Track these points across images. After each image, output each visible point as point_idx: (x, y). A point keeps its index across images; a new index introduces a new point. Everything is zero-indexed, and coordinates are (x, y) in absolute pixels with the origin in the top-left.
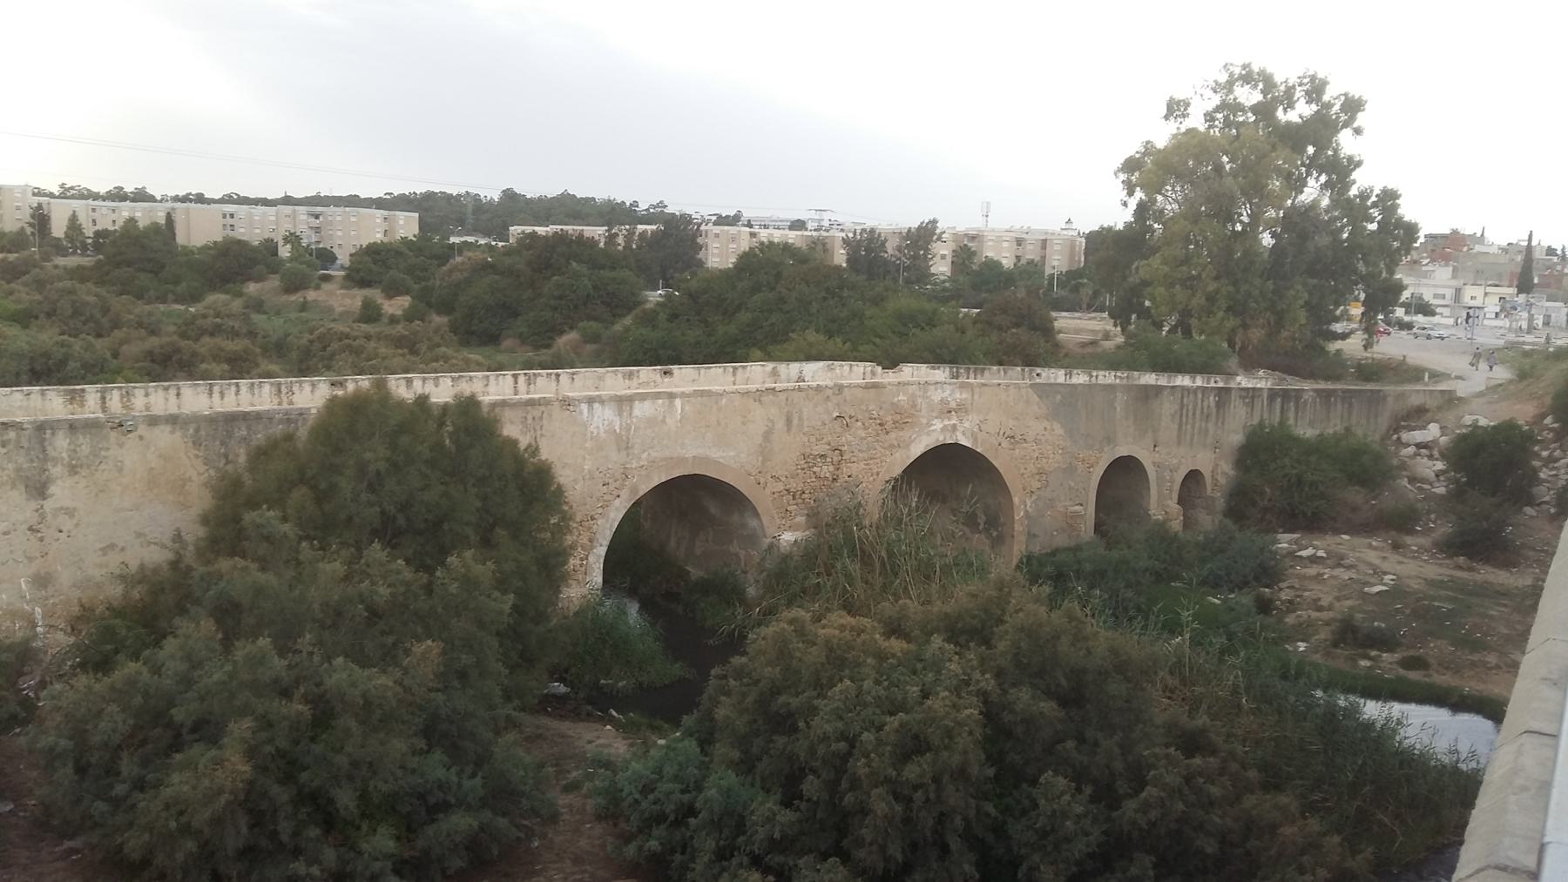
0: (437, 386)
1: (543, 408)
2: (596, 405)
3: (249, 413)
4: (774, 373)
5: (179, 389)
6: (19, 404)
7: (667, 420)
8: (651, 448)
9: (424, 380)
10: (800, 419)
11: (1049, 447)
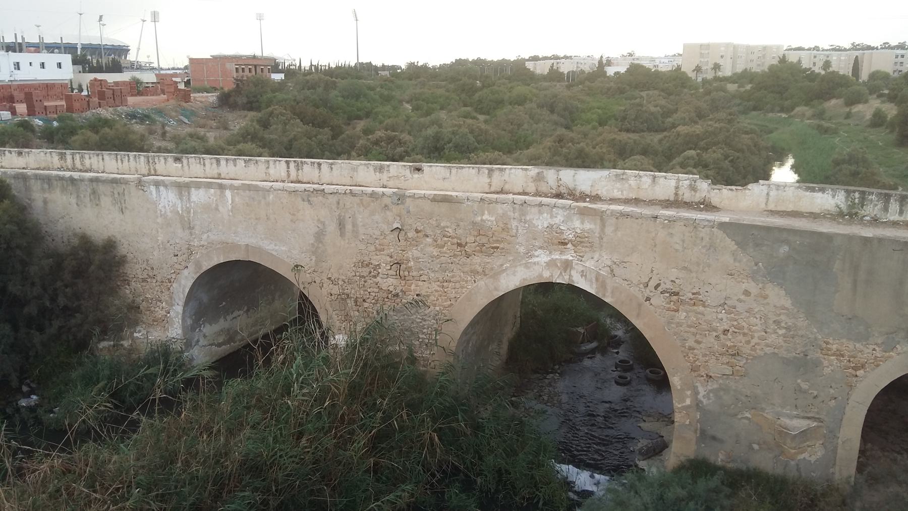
0: (235, 166)
1: (124, 186)
3: (842, 185)
4: (539, 178)
5: (103, 156)
6: (42, 158)
7: (220, 208)
9: (227, 160)
10: (354, 225)
11: (753, 320)
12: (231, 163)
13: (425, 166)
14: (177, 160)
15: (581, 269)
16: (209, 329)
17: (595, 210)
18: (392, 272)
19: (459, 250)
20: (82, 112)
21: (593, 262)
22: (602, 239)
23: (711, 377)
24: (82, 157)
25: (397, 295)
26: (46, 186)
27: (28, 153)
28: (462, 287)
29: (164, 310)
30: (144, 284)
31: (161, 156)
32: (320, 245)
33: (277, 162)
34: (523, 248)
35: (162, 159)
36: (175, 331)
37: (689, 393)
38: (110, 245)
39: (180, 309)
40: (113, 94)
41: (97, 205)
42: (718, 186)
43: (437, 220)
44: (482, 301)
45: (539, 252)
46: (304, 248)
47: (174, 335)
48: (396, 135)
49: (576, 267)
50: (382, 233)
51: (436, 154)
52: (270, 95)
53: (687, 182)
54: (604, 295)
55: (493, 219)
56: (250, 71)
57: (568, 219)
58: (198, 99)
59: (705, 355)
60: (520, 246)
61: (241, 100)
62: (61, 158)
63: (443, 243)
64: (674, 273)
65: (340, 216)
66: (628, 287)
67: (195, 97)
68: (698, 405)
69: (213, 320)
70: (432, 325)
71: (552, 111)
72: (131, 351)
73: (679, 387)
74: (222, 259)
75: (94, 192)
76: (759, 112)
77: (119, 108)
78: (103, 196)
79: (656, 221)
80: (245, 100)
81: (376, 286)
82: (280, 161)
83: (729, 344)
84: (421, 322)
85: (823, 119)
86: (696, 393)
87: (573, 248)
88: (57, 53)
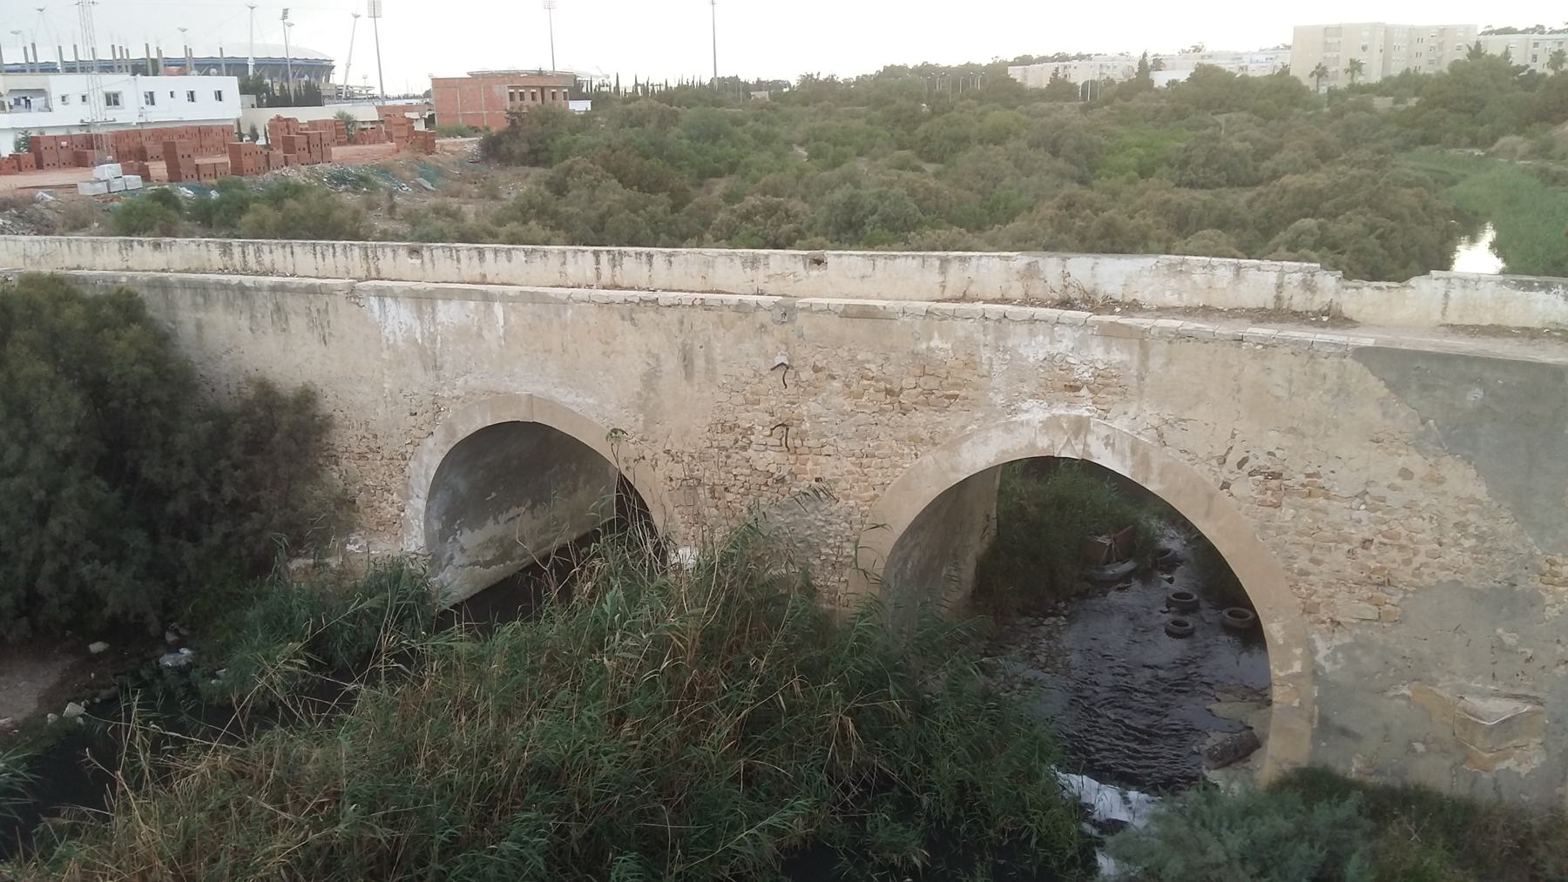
0: (509, 261)
1: (326, 298)
2: (388, 301)
5: (292, 247)
7: (485, 333)
8: (466, 373)
9: (496, 251)
10: (709, 360)
11: (1417, 522)
12: (502, 257)
13: (830, 255)
14: (414, 252)
15: (1104, 432)
16: (469, 538)
17: (1130, 327)
18: (774, 441)
19: (888, 401)
20: (257, 174)
21: (1126, 421)
22: (1143, 379)
23: (1339, 623)
24: (258, 251)
25: (782, 480)
26: (200, 300)
27: (170, 244)
28: (895, 466)
29: (395, 505)
30: (361, 462)
31: (387, 246)
32: (652, 395)
33: (579, 254)
34: (1001, 396)
35: (388, 251)
36: (414, 541)
37: (1298, 651)
38: (306, 398)
39: (420, 503)
40: (308, 143)
41: (284, 330)
42: (1356, 283)
43: (850, 349)
44: (930, 491)
45: (1030, 403)
46: (626, 401)
47: (413, 548)
48: (780, 204)
49: (1096, 429)
50: (756, 373)
51: (850, 234)
52: (566, 138)
53: (1298, 276)
54: (1146, 479)
55: (949, 346)
56: (533, 96)
57: (1082, 344)
58: (447, 148)
59: (1328, 585)
60: (996, 393)
61: (520, 148)
62: (224, 253)
63: (861, 390)
64: (1273, 439)
65: (684, 345)
66: (1188, 464)
67: (442, 145)
68: (1315, 673)
69: (476, 522)
70: (843, 532)
71: (1055, 153)
72: (341, 574)
73: (1281, 642)
74: (489, 419)
75: (278, 309)
76: (1432, 147)
77: (317, 167)
78: (293, 316)
79: (1240, 347)
80: (525, 147)
81: (748, 464)
82: (583, 251)
83: (1373, 564)
84: (823, 527)
85: (1550, 158)
86: (1313, 652)
87: (1091, 395)
88: (214, 75)
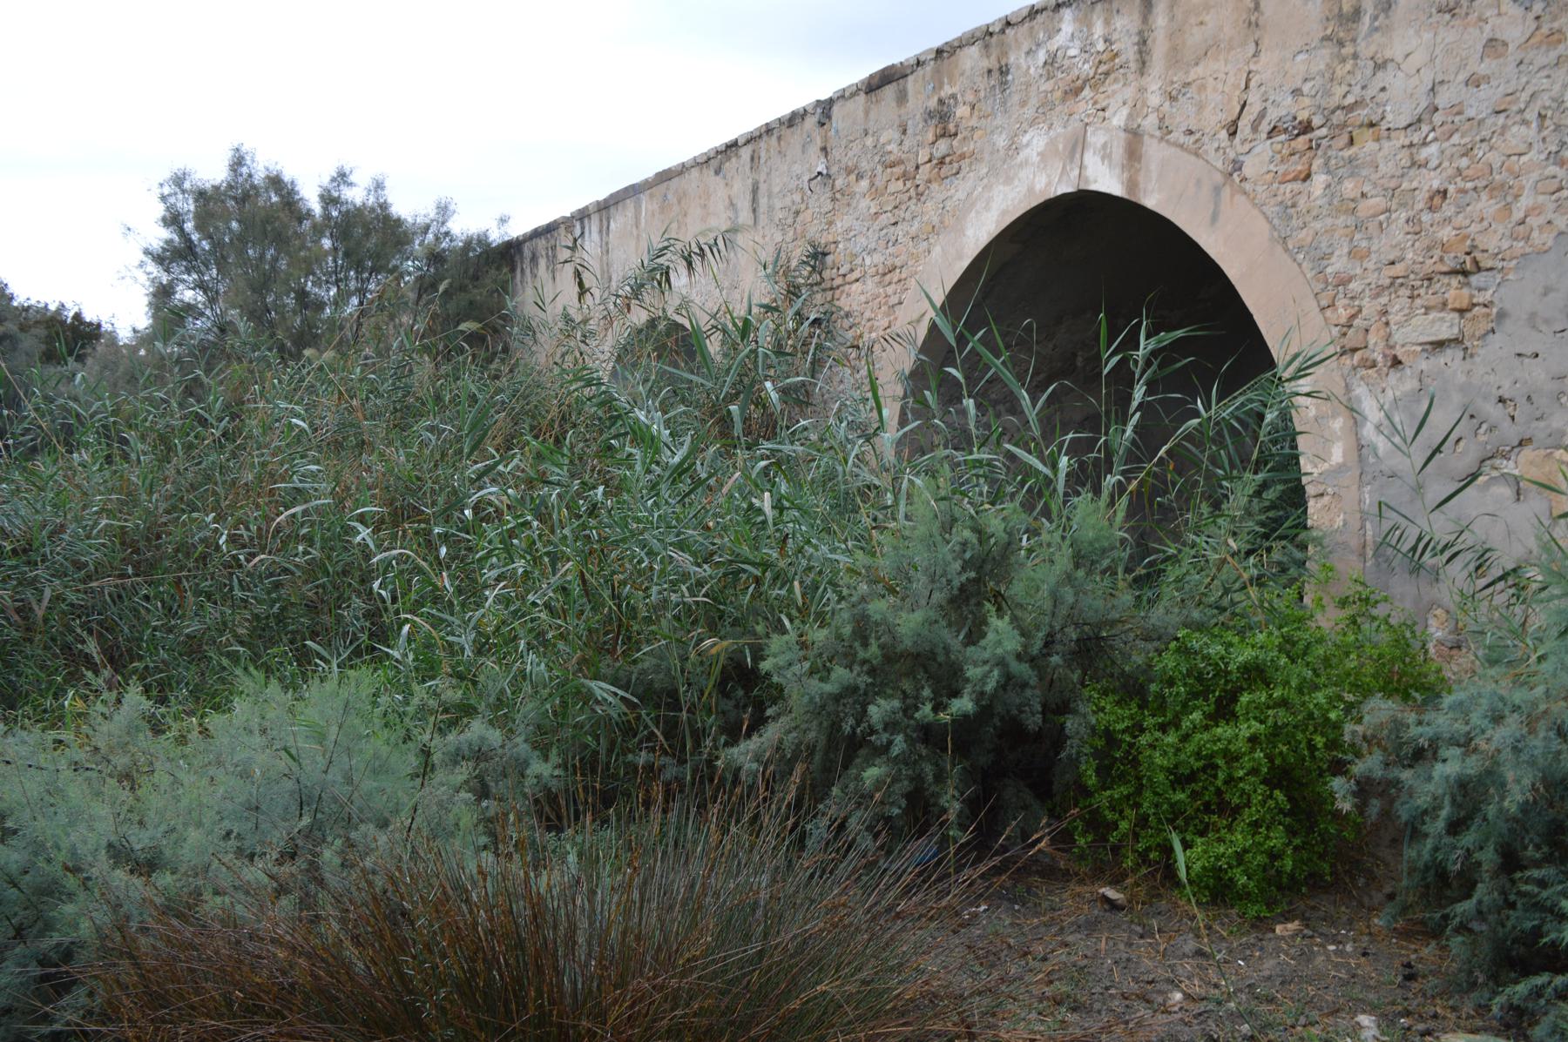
37: (1338, 424)
59: (1380, 290)
83: (1446, 233)
